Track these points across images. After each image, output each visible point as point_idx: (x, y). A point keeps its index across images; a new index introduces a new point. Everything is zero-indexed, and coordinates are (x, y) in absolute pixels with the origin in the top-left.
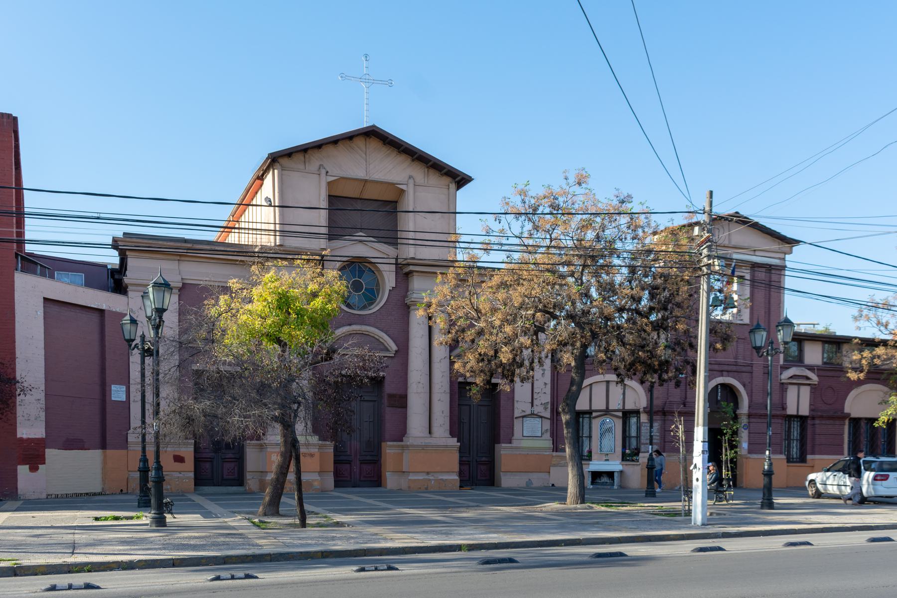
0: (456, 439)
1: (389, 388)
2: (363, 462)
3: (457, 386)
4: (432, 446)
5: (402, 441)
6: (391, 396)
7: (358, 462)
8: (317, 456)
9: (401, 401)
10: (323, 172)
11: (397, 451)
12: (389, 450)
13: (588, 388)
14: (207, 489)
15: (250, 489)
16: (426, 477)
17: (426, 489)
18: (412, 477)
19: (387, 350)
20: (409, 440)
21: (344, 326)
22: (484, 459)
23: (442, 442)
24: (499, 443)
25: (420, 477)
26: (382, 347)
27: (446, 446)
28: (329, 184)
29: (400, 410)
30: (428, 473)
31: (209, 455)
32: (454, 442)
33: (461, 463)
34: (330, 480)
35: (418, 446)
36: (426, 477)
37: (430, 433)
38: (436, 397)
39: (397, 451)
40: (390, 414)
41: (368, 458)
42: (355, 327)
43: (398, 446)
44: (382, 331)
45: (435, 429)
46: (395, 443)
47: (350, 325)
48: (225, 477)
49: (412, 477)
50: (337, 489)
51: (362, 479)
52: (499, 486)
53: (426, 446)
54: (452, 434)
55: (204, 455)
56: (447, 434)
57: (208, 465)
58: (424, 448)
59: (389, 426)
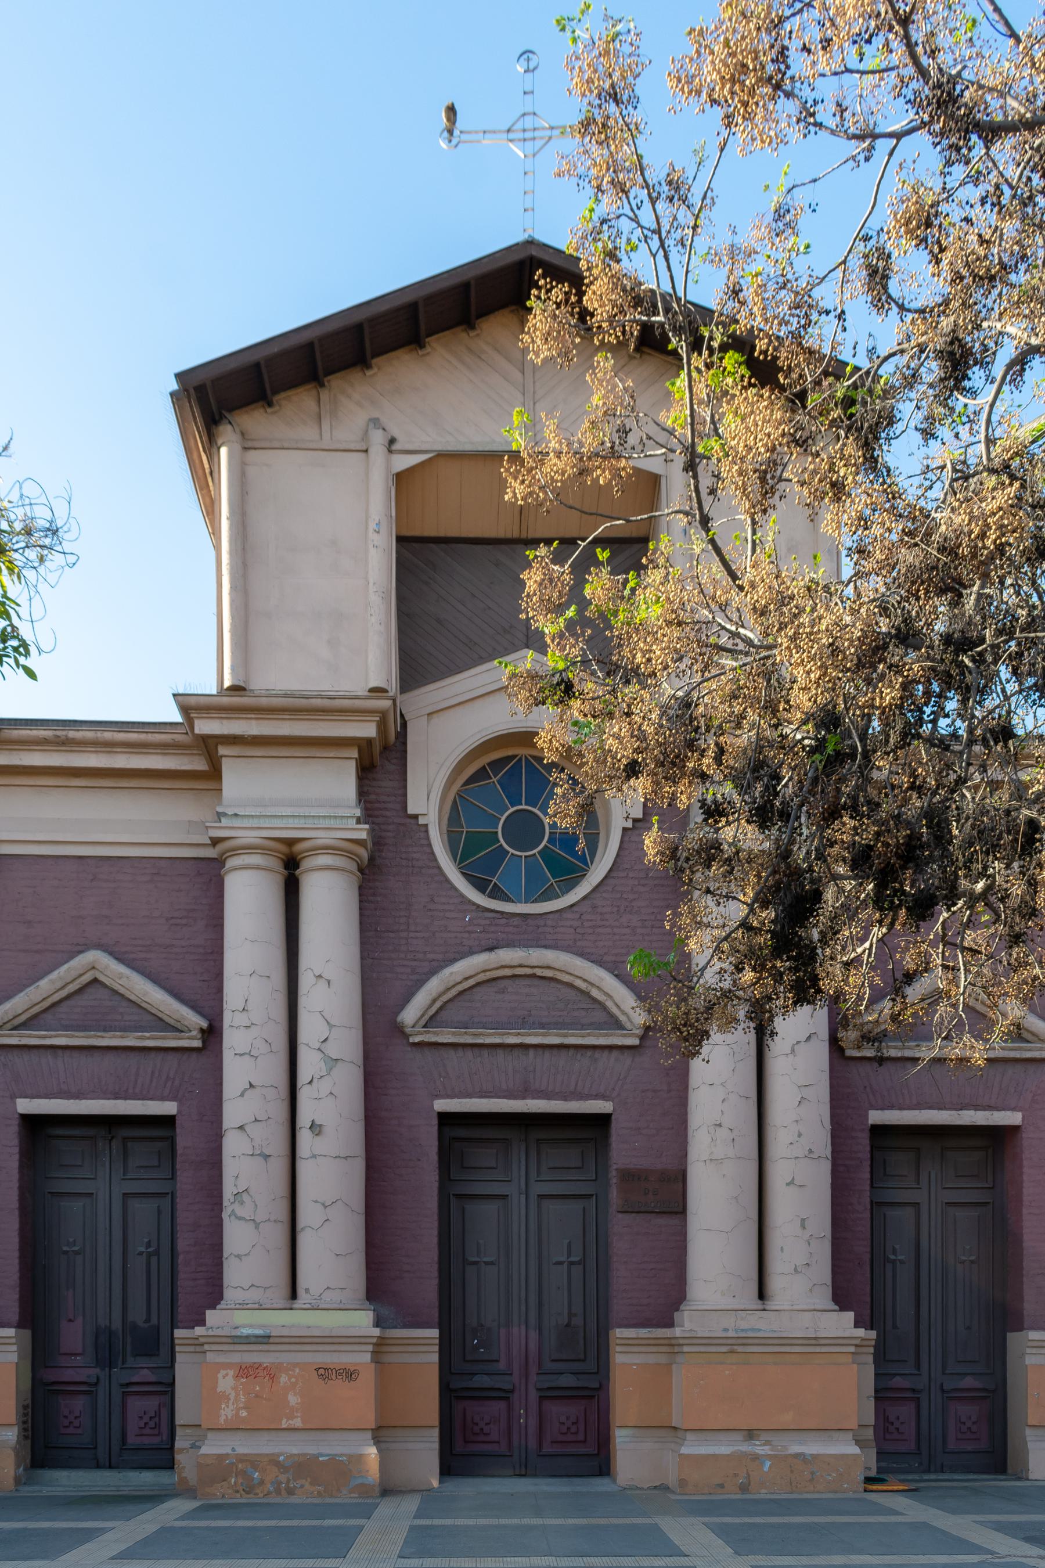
0: (850, 1315)
1: (624, 1150)
2: (548, 1395)
3: (864, 1141)
4: (764, 1341)
5: (670, 1324)
6: (629, 1176)
7: (533, 1395)
8: (368, 1377)
9: (666, 1194)
10: (378, 439)
11: (651, 1359)
12: (629, 1353)
13: (654, 252)
14: (67, 1481)
15: (183, 1480)
16: (745, 1448)
17: (744, 1488)
18: (693, 1447)
19: (618, 1025)
20: (689, 1322)
21: (471, 952)
22: (969, 1382)
23: (800, 1326)
24: (1019, 1327)
25: (723, 1448)
26: (599, 1016)
27: (815, 1341)
28: (402, 480)
29: (662, 1221)
30: (750, 1434)
31: (82, 1375)
32: (842, 1324)
33: (883, 1395)
34: (424, 1454)
35: (710, 1341)
36: (745, 1448)
37: (762, 1295)
38: (779, 1173)
39: (651, 1359)
40: (628, 1237)
41: (567, 1381)
42: (507, 956)
43: (656, 1342)
44: (600, 963)
45: (777, 1283)
46: (643, 1332)
47: (491, 949)
48: (132, 1440)
49: (693, 1447)
50: (468, 1488)
51: (547, 1449)
52: (1021, 1475)
53: (743, 1341)
54: (841, 1299)
55: (69, 1375)
56: (824, 1298)
57: (79, 1404)
58: (736, 1346)
59: (624, 1278)
